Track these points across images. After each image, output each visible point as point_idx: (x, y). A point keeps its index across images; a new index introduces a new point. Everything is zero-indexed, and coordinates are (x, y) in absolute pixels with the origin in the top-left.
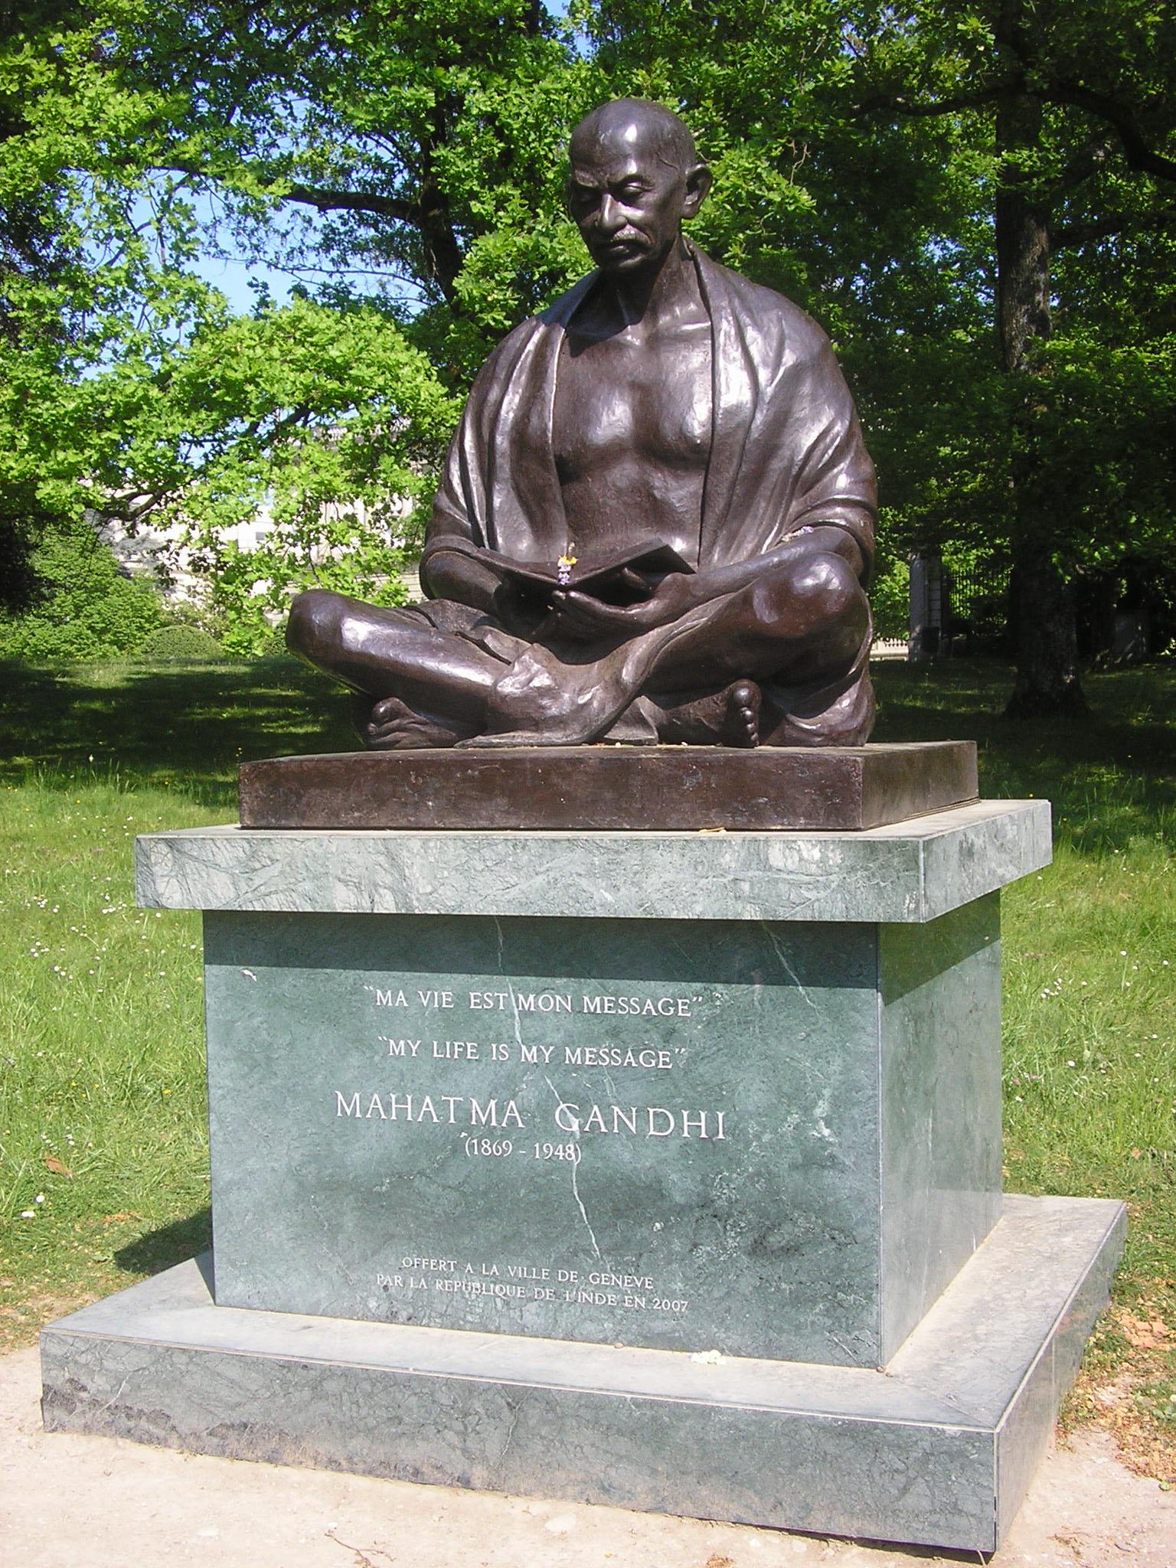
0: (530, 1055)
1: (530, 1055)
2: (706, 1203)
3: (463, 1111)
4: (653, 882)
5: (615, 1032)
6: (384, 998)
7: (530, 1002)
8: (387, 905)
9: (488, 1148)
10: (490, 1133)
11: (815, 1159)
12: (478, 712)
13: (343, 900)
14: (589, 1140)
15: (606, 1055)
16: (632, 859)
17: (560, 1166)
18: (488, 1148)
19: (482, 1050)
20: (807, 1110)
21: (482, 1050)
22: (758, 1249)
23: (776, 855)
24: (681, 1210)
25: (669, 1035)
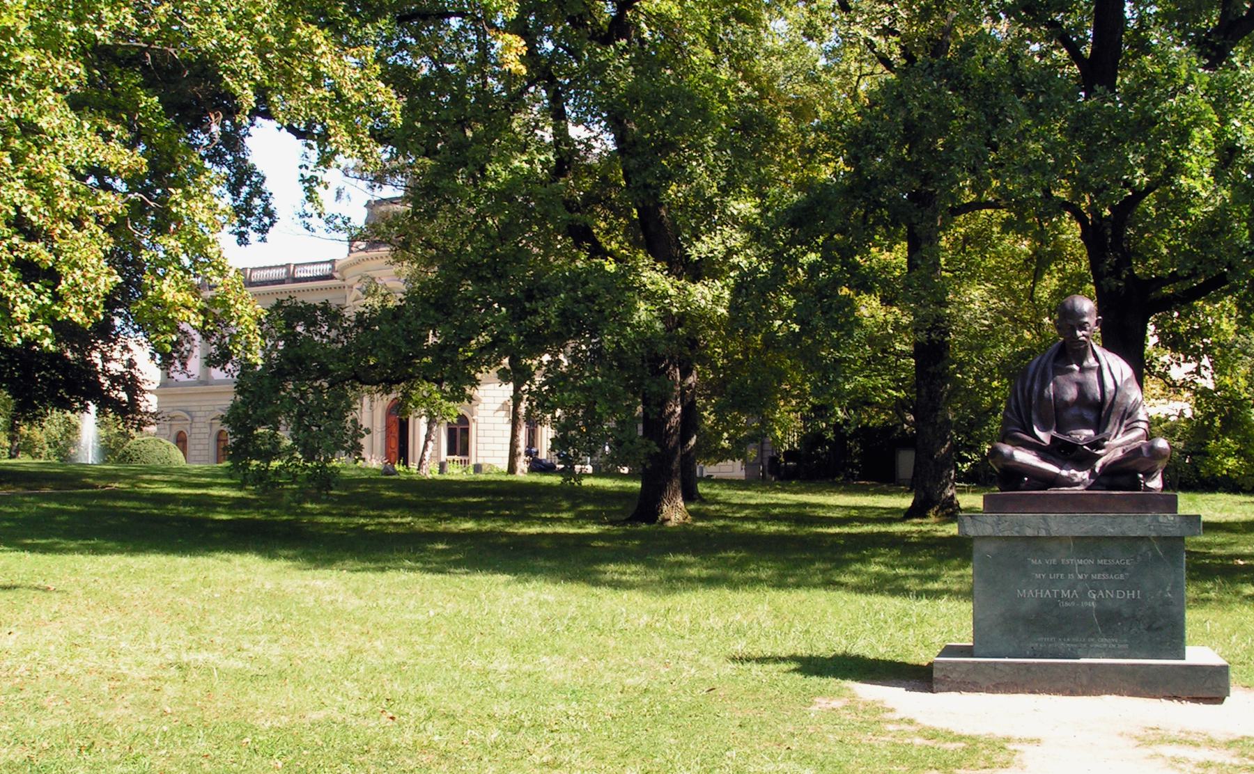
0: (1081, 577)
1: (1081, 577)
2: (1134, 616)
3: (1059, 594)
4: (1125, 527)
5: (1107, 569)
6: (1034, 562)
7: (1081, 562)
8: (1043, 533)
9: (1067, 604)
10: (1067, 599)
11: (1167, 603)
12: (1069, 482)
13: (1029, 532)
14: (1098, 601)
15: (1105, 576)
16: (1119, 520)
17: (1088, 608)
18: (1067, 604)
19: (1066, 576)
20: (1164, 589)
21: (1066, 576)
22: (1149, 629)
23: (1161, 519)
24: (1126, 619)
25: (1124, 570)
